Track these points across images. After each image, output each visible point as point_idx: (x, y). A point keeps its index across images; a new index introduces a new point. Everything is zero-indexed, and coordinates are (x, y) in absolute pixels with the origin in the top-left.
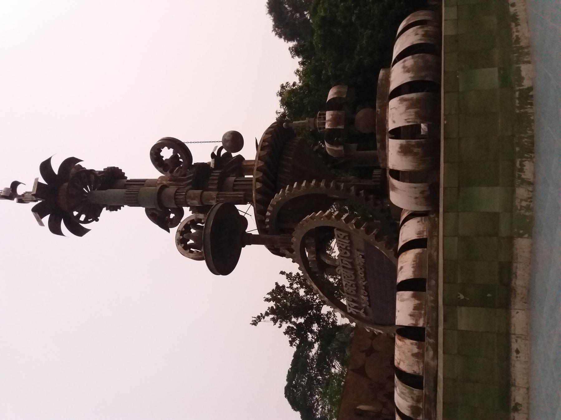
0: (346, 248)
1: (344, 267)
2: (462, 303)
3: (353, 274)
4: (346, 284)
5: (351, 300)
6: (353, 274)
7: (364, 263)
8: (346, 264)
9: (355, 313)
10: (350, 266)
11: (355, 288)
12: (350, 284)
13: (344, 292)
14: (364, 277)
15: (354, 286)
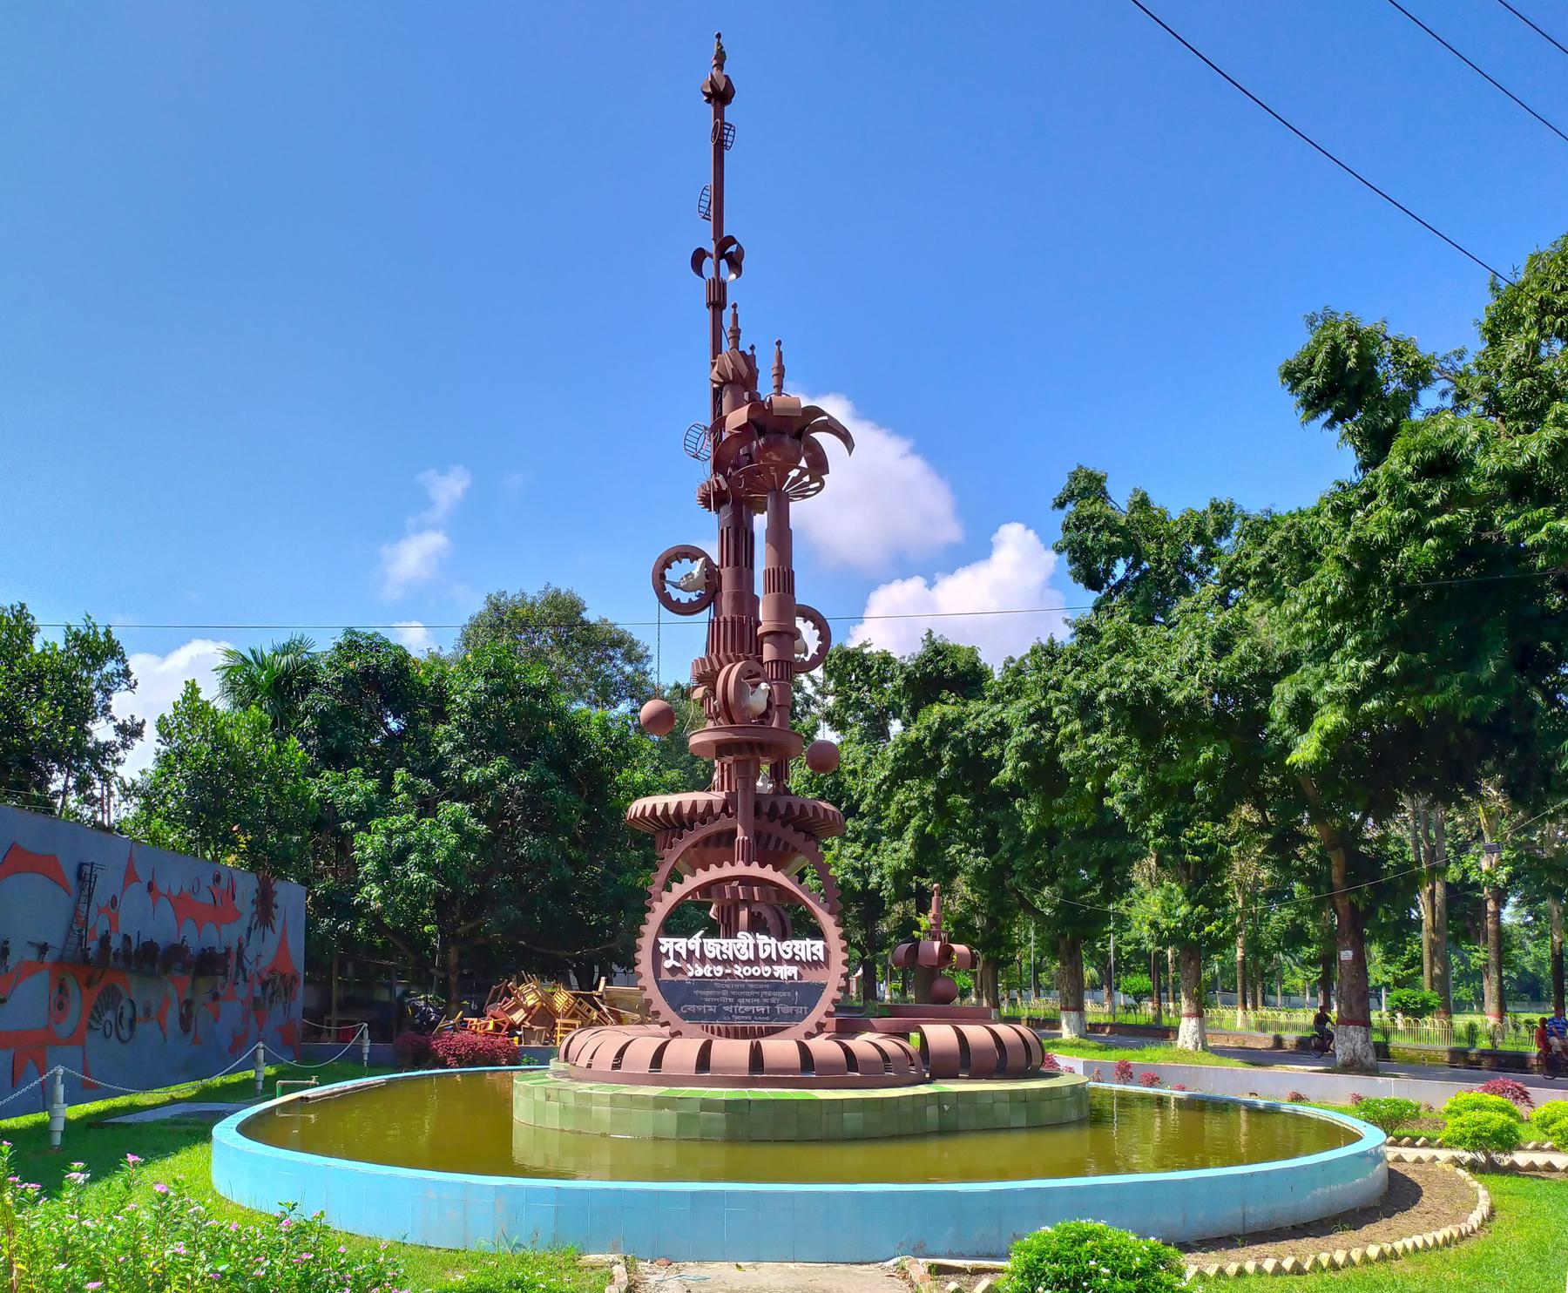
0: (794, 954)
1: (756, 946)
2: (940, 1108)
3: (749, 959)
4: (722, 945)
5: (691, 948)
6: (749, 959)
7: (779, 978)
8: (764, 951)
9: (663, 950)
10: (763, 956)
11: (719, 958)
12: (724, 950)
13: (701, 937)
14: (752, 975)
15: (725, 957)
